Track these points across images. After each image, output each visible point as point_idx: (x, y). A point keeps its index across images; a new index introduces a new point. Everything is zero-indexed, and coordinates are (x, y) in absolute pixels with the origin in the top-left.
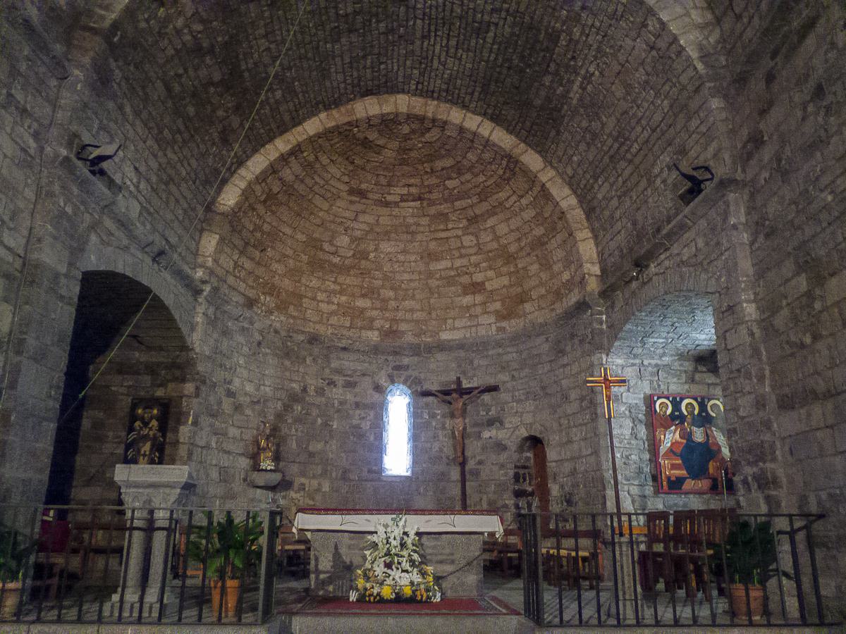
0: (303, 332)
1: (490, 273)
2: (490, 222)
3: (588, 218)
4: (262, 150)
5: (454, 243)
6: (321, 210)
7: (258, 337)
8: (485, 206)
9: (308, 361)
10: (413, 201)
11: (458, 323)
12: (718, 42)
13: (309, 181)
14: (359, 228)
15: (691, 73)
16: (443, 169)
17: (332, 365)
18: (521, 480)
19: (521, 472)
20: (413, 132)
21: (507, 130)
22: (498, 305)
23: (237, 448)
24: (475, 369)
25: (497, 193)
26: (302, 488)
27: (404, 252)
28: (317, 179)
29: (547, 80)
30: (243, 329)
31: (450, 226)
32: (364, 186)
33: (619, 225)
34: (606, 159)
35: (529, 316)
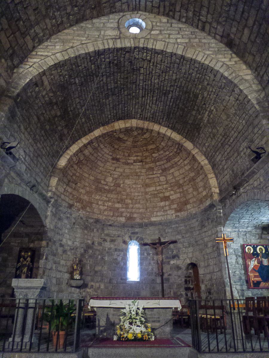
0: (92, 218)
1: (172, 192)
2: (171, 171)
3: (213, 168)
4: (76, 143)
5: (156, 180)
6: (101, 167)
7: (73, 221)
8: (169, 164)
9: (95, 230)
10: (139, 162)
11: (159, 214)
12: (264, 97)
13: (95, 155)
15: (253, 109)
17: (105, 232)
18: (188, 283)
20: (139, 134)
21: (178, 133)
22: (175, 206)
23: (65, 269)
24: (166, 234)
25: (174, 159)
27: (135, 184)
28: (99, 154)
29: (194, 113)
30: (67, 218)
31: (155, 173)
32: (118, 157)
33: (226, 172)
34: (220, 145)
35: (189, 210)
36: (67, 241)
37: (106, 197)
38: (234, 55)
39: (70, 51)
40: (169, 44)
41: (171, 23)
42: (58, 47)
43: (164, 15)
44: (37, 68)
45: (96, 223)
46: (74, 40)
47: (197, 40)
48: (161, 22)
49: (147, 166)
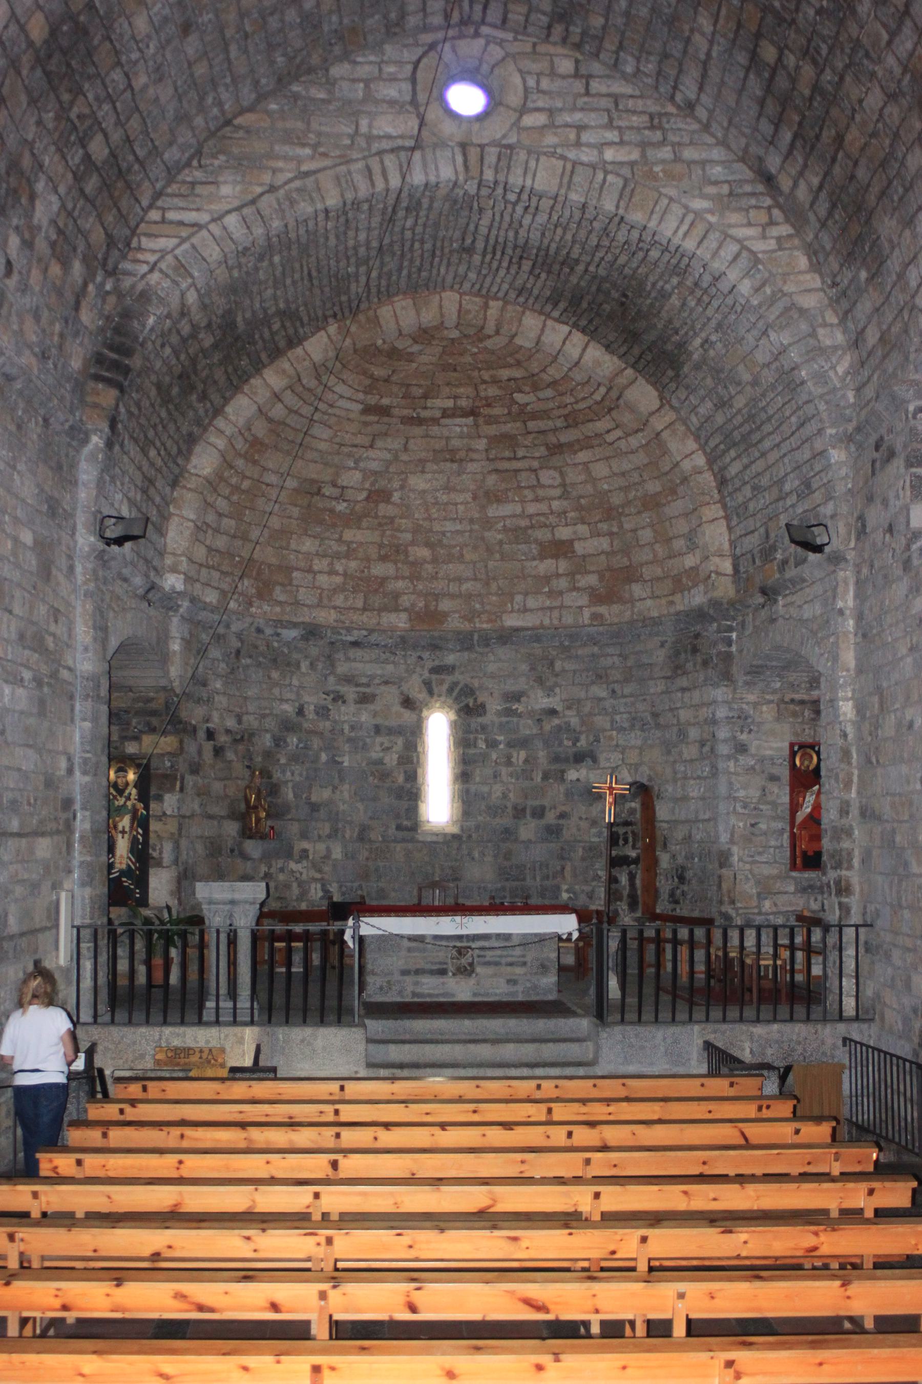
0: (295, 625)
1: (583, 529)
2: (582, 456)
5: (525, 479)
7: (235, 644)
9: (304, 666)
11: (531, 603)
14: (375, 459)
16: (509, 380)
18: (621, 842)
19: (621, 830)
21: (607, 347)
24: (557, 675)
26: (304, 854)
27: (448, 488)
31: (521, 453)
32: (385, 401)
36: (222, 718)
37: (340, 540)
38: (776, 212)
39: (267, 203)
40: (579, 169)
41: (589, 77)
42: (226, 190)
43: (564, 40)
44: (170, 272)
45: (307, 640)
46: (278, 158)
47: (666, 153)
48: (553, 74)
49: (492, 430)
